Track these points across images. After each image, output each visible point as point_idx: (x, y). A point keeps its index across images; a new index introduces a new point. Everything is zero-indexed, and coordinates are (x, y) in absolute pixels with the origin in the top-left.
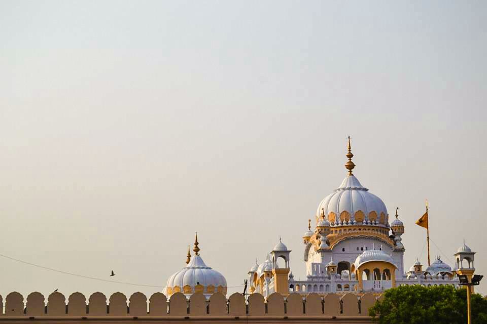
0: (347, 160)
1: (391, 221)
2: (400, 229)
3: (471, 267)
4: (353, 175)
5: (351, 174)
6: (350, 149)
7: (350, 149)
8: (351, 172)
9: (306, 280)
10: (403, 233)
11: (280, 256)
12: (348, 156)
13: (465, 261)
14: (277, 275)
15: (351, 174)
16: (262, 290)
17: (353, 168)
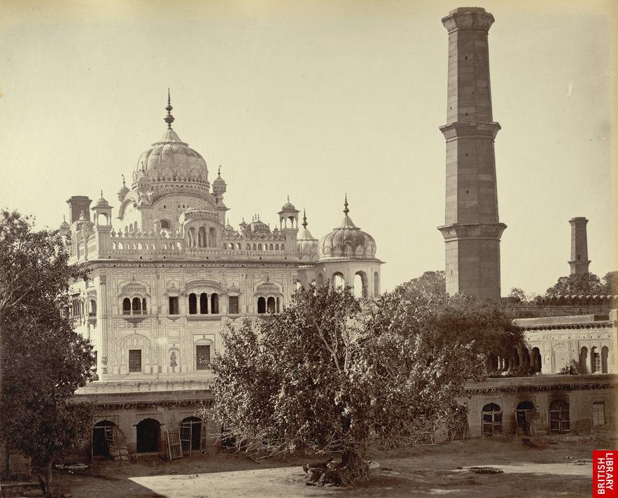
0: (166, 113)
1: (212, 178)
2: (220, 187)
3: (295, 227)
4: (171, 129)
5: (170, 128)
6: (169, 101)
7: (169, 101)
8: (170, 126)
9: (593, 269)
10: (225, 191)
11: (102, 213)
12: (167, 109)
13: (289, 220)
14: (100, 236)
15: (170, 128)
16: (78, 249)
17: (172, 121)
